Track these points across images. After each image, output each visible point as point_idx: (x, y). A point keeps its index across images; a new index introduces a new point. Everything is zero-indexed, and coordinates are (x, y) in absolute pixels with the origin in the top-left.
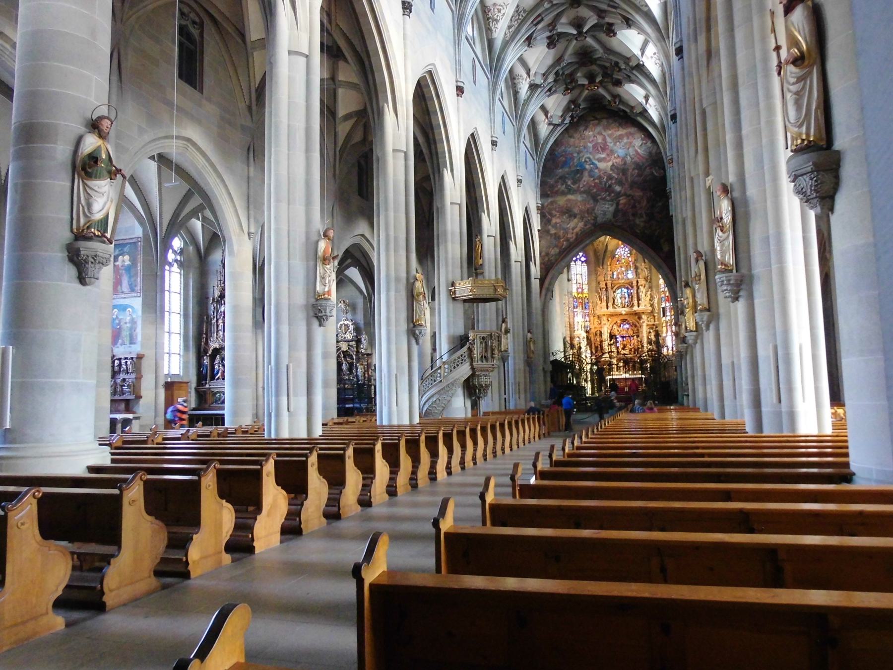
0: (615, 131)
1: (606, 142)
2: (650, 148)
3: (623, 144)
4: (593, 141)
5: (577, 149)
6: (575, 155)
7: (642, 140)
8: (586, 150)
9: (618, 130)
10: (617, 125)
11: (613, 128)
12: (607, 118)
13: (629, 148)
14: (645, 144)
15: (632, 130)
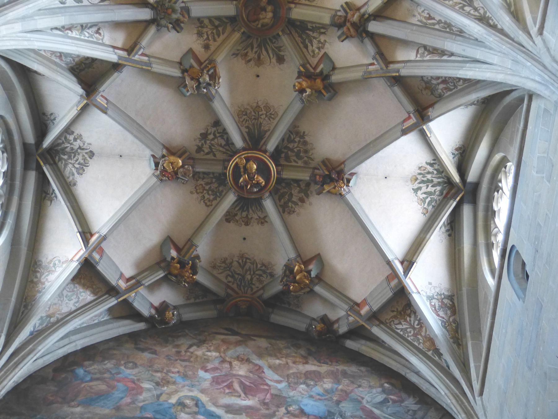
0: (294, 363)
1: (261, 378)
2: (415, 412)
3: (318, 389)
4: (215, 369)
5: (159, 375)
6: (146, 385)
7: (384, 391)
8: (187, 382)
9: (307, 363)
10: (303, 352)
11: (287, 356)
12: (266, 337)
13: (338, 403)
14: (394, 402)
15: (352, 369)
